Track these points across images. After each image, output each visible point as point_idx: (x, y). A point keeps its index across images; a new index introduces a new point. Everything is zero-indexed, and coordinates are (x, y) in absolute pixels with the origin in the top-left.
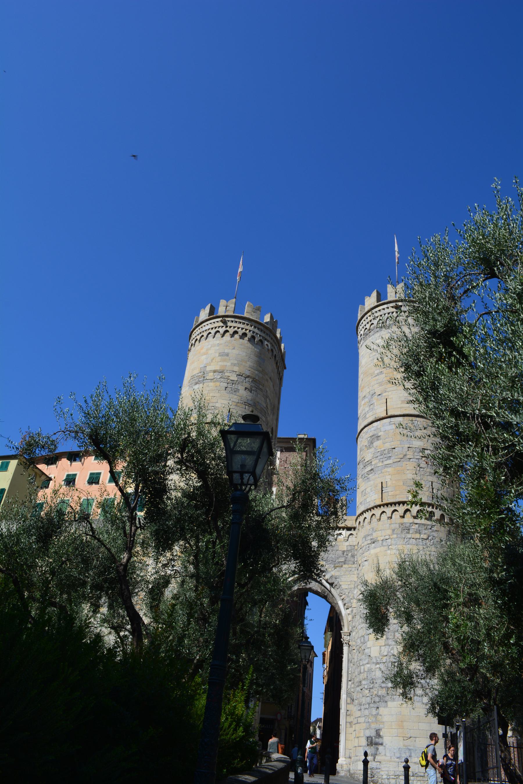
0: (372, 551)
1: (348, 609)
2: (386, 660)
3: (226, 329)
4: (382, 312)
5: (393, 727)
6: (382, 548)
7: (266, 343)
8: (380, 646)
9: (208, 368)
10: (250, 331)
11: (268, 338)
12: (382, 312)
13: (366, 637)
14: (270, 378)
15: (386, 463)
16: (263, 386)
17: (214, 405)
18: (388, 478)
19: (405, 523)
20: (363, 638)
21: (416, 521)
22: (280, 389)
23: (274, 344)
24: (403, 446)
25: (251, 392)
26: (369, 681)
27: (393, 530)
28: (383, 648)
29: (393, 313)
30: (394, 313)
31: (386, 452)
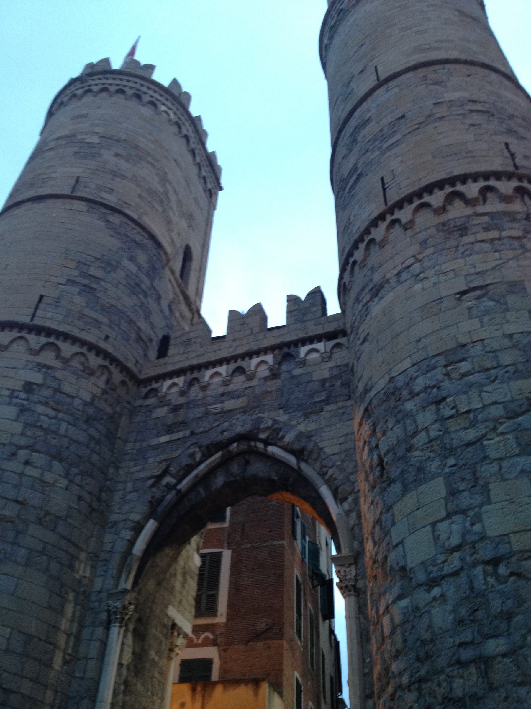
0: (376, 308)
1: (345, 499)
2: (462, 560)
6: (400, 286)
7: (163, 108)
8: (434, 525)
10: (131, 88)
14: (175, 160)
15: (385, 145)
16: (157, 161)
19: (454, 219)
20: (377, 528)
21: (480, 209)
25: (127, 161)
26: (412, 654)
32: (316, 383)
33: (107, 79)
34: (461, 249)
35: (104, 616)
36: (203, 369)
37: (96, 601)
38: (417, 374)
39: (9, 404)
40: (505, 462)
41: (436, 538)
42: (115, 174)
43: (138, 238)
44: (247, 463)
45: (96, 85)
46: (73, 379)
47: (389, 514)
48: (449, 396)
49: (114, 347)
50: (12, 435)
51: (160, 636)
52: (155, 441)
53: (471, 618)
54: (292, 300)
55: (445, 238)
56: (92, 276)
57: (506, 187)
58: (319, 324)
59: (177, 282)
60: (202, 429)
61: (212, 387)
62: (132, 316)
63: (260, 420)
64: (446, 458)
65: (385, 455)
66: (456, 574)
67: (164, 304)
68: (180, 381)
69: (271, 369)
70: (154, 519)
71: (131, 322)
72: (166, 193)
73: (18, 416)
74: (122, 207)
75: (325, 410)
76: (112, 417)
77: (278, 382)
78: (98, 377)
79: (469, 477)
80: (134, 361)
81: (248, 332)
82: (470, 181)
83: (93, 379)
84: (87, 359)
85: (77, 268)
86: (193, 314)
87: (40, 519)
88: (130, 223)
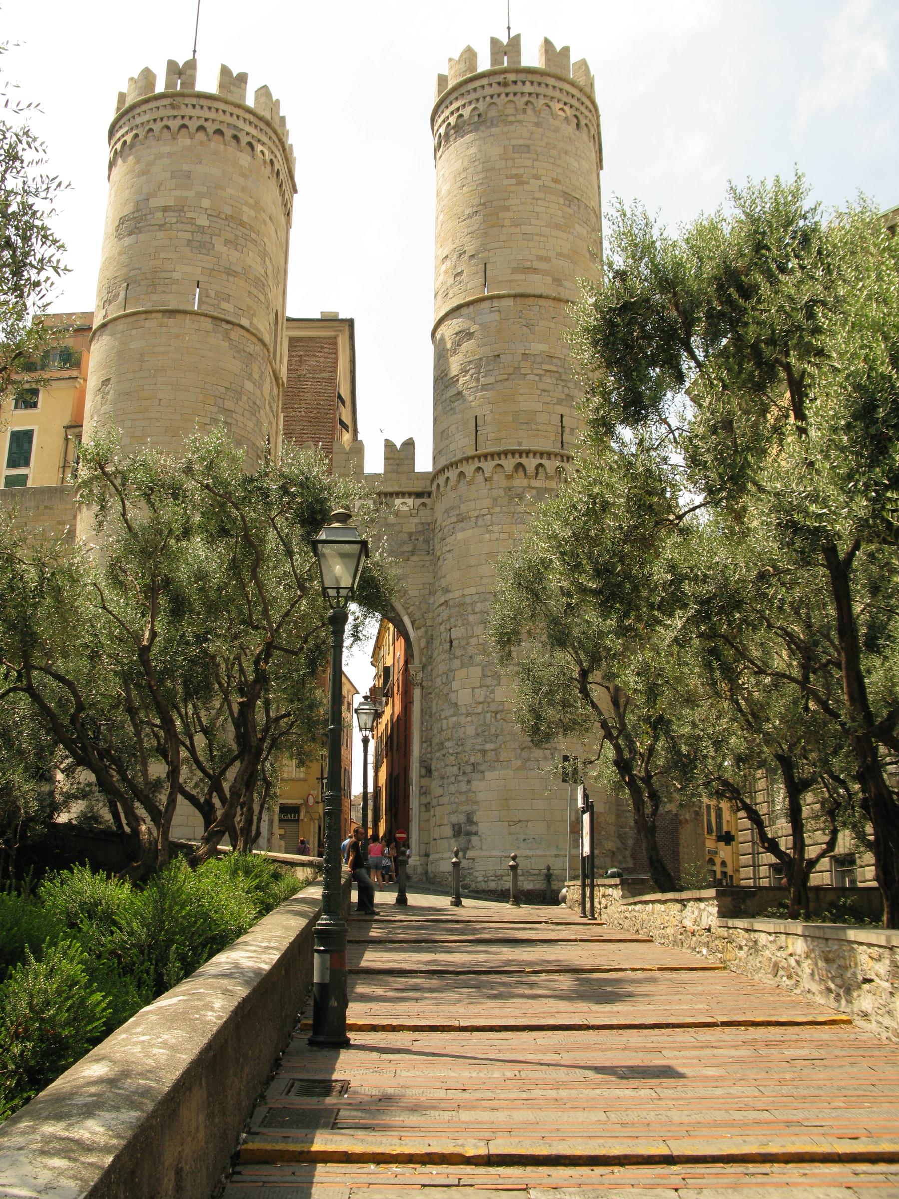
0: (460, 535)
3: (182, 122)
4: (479, 94)
8: (473, 689)
9: (154, 203)
11: (264, 139)
12: (479, 94)
13: (451, 675)
14: (271, 219)
17: (168, 275)
22: (287, 233)
23: (274, 149)
27: (495, 500)
29: (499, 95)
30: (503, 96)
41: (474, 696)
42: (229, 272)
54: (389, 445)
82: (531, 455)
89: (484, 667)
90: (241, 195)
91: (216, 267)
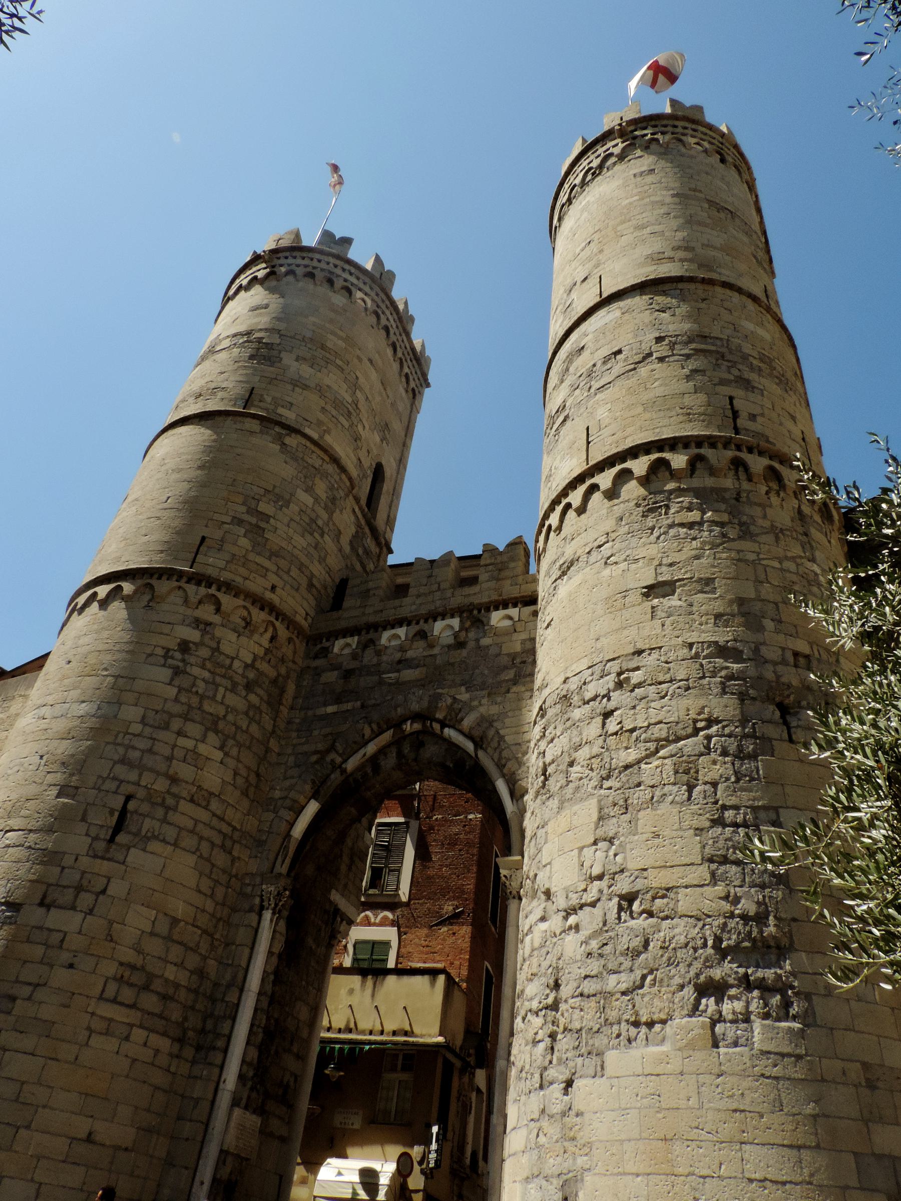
2: (601, 891)
5: (631, 1167)
7: (359, 294)
8: (581, 849)
10: (322, 270)
14: (370, 361)
15: (596, 385)
18: (602, 413)
24: (641, 338)
28: (588, 852)
31: (599, 364)
32: (506, 658)
33: (295, 258)
34: (656, 533)
35: (257, 901)
36: (380, 629)
37: (249, 885)
38: (591, 678)
39: (164, 666)
40: (658, 789)
42: (297, 383)
43: (318, 463)
44: (421, 744)
45: (281, 265)
46: (233, 636)
47: (544, 830)
48: (616, 709)
49: (281, 599)
50: (166, 700)
51: (320, 922)
52: (321, 711)
53: (600, 951)
55: (643, 516)
56: (261, 513)
57: (719, 457)
58: (517, 584)
59: (362, 511)
60: (373, 702)
61: (389, 651)
62: (304, 559)
63: (438, 697)
64: (603, 779)
65: (550, 764)
66: (593, 905)
67: (345, 540)
68: (354, 641)
69: (456, 635)
70: (316, 800)
71: (301, 567)
72: (356, 404)
73: (172, 679)
74: (302, 425)
75: (512, 691)
76: (274, 682)
77: (464, 652)
78: (261, 634)
79: (621, 802)
80: (304, 615)
81: (435, 587)
83: (256, 637)
84: (249, 613)
85: (244, 504)
86: (381, 549)
87: (193, 796)
88: (308, 444)
89: (599, 801)
90: (327, 325)
91: (279, 377)
